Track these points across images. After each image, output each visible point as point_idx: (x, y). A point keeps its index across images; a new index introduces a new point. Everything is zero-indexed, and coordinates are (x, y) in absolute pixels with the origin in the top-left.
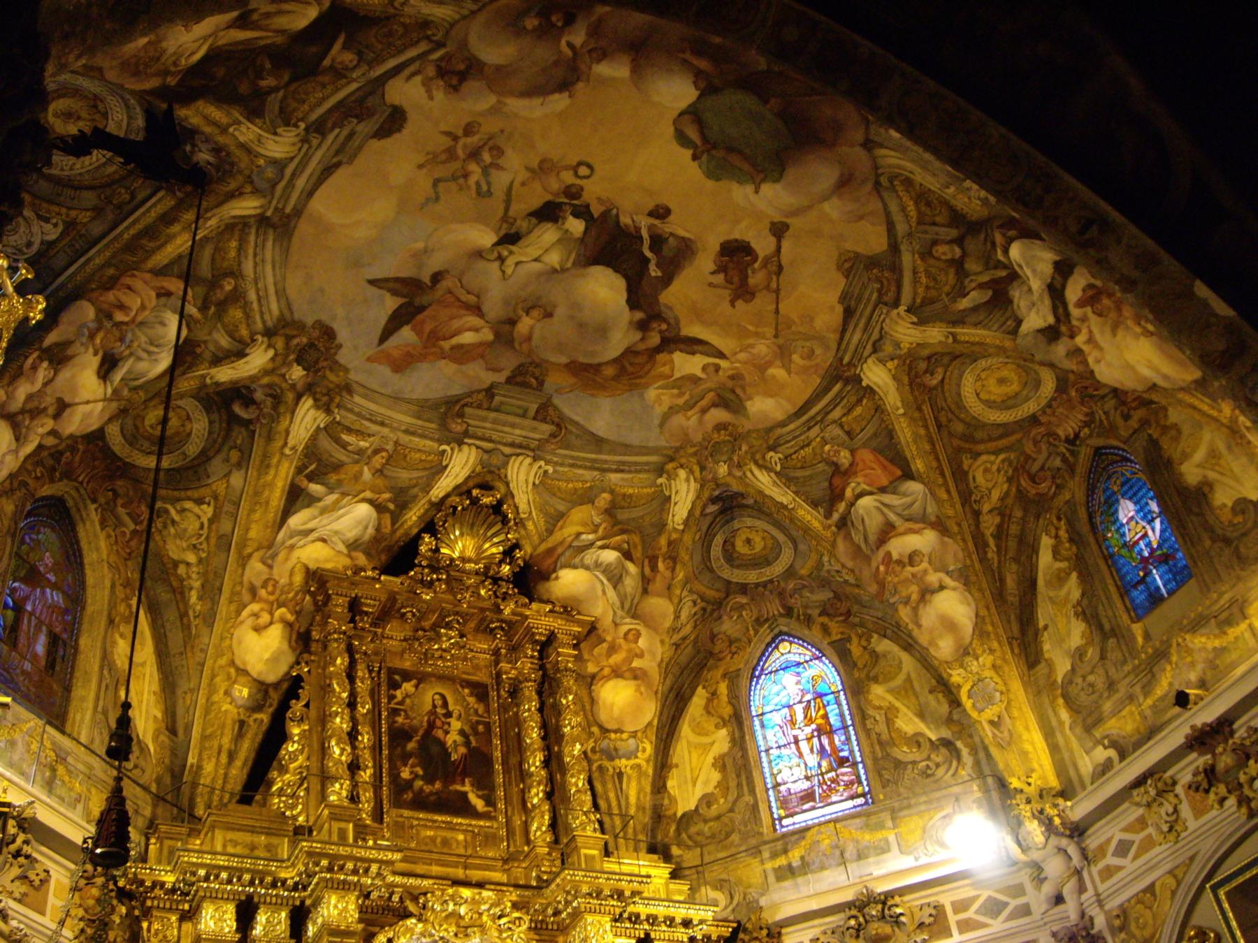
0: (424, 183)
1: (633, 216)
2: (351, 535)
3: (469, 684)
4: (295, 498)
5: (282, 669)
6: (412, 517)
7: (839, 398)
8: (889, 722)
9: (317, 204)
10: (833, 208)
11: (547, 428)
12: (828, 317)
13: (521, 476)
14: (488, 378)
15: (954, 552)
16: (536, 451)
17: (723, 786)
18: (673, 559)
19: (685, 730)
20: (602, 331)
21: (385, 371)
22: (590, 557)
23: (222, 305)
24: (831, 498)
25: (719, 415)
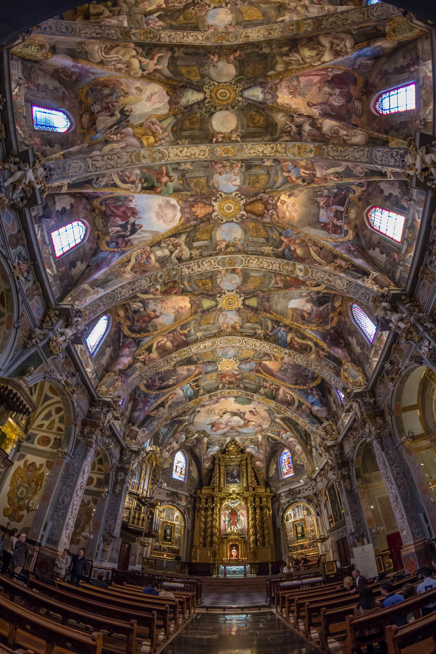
0: (207, 415)
1: (235, 411)
4: (208, 448)
6: (224, 446)
9: (195, 420)
10: (259, 405)
12: (267, 415)
13: (237, 439)
15: (296, 440)
16: (238, 436)
20: (239, 422)
24: (279, 435)
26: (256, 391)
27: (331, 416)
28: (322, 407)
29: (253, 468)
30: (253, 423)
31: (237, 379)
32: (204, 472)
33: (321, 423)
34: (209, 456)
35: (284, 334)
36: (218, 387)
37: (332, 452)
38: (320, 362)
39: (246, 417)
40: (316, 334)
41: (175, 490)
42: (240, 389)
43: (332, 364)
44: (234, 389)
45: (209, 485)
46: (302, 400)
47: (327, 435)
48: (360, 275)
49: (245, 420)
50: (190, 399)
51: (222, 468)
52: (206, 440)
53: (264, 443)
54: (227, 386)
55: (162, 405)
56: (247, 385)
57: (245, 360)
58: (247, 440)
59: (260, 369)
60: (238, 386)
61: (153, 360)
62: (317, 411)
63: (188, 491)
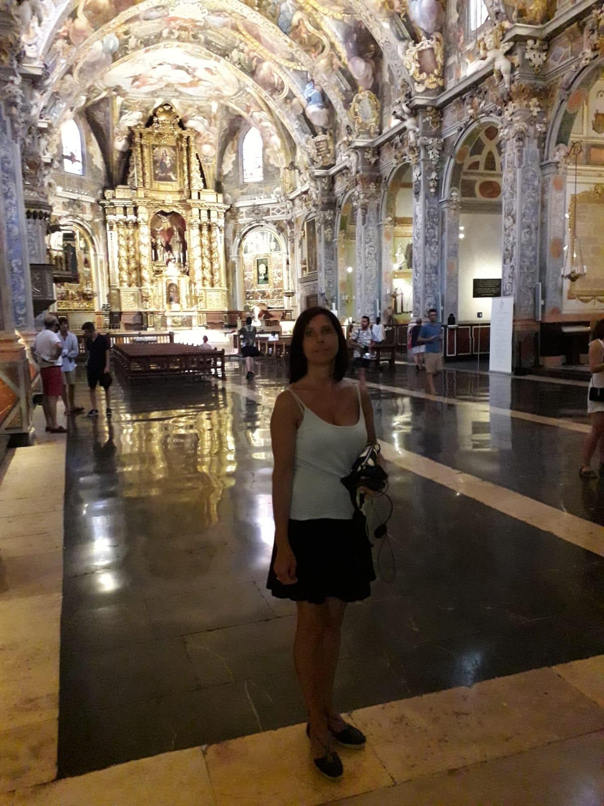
1: (181, 64)
2: (137, 118)
3: (172, 147)
4: (121, 114)
5: (127, 148)
6: (151, 113)
7: (243, 94)
8: (268, 160)
11: (177, 94)
13: (175, 102)
14: (160, 87)
15: (274, 128)
16: (177, 97)
17: (233, 169)
18: (215, 118)
19: (227, 151)
21: (135, 89)
22: (196, 118)
23: (93, 91)
24: (248, 111)
25: (217, 92)
26: (224, 53)
27: (331, 126)
28: (322, 107)
29: (197, 155)
30: (208, 84)
31: (196, 26)
32: (116, 157)
33: (315, 134)
34: (122, 129)
35: (291, 9)
36: (161, 33)
37: (319, 183)
38: (329, 77)
39: (196, 74)
40: (338, 27)
41: (75, 196)
42: (199, 43)
43: (345, 85)
44: (191, 42)
45: (124, 182)
46: (295, 92)
47: (318, 156)
48: (407, 34)
49: (194, 77)
50: (115, 57)
51: (146, 151)
52: (119, 100)
53: (219, 115)
54: (177, 33)
55: (70, 72)
56: (210, 38)
57: (219, 12)
58: (190, 106)
59: (239, 23)
60: (195, 36)
61: (81, 34)
62: (314, 113)
63: (93, 194)
